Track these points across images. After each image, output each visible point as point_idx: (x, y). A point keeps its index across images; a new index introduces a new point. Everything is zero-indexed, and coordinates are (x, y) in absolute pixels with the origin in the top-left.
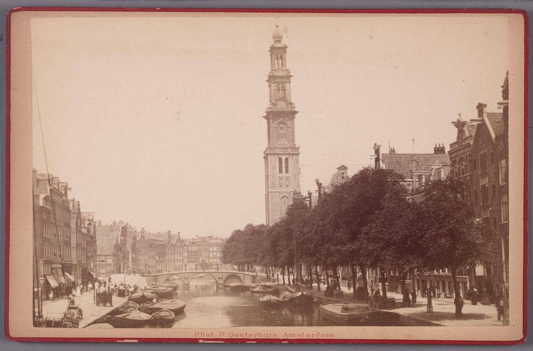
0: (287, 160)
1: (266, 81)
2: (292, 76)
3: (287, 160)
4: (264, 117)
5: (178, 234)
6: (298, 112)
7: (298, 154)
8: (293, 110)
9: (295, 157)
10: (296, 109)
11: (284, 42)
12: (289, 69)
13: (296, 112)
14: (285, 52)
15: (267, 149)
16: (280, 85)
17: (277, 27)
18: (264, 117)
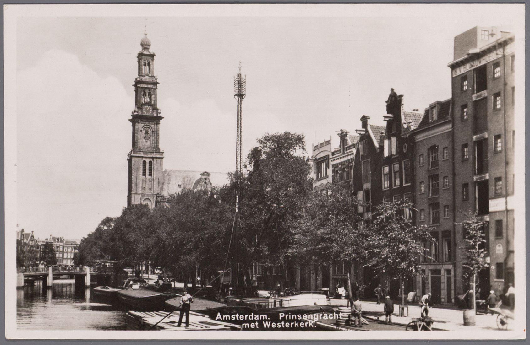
0: (150, 163)
1: (133, 85)
2: (159, 83)
3: (150, 163)
4: (129, 120)
5: (31, 233)
6: (163, 118)
7: (162, 158)
8: (159, 115)
9: (159, 160)
10: (161, 115)
11: (152, 50)
12: (156, 76)
13: (161, 118)
14: (153, 60)
15: (131, 152)
16: (147, 90)
17: (146, 35)
18: (129, 120)
